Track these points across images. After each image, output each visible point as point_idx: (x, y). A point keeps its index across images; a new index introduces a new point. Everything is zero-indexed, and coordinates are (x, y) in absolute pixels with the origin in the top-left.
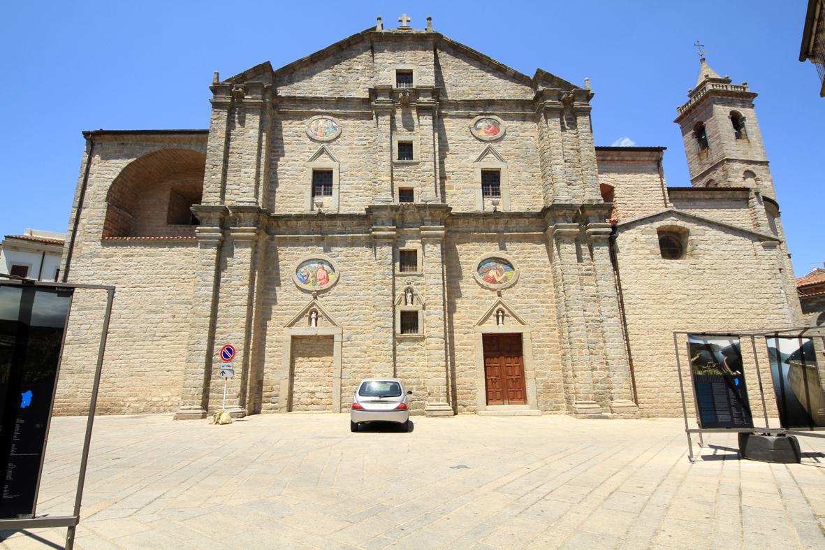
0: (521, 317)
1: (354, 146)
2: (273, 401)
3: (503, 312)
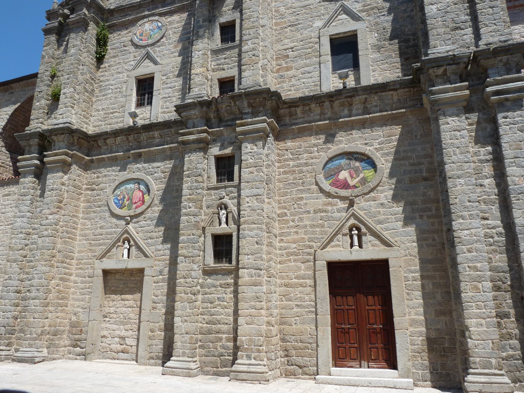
0: (386, 234)
2: (82, 345)
3: (359, 229)
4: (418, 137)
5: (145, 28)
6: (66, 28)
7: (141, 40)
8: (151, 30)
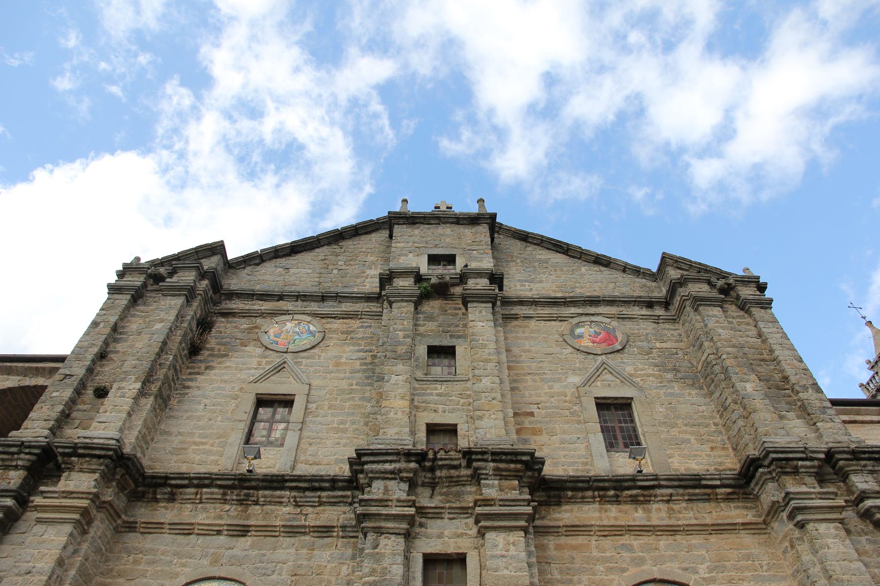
1: (343, 360)
4: (765, 568)
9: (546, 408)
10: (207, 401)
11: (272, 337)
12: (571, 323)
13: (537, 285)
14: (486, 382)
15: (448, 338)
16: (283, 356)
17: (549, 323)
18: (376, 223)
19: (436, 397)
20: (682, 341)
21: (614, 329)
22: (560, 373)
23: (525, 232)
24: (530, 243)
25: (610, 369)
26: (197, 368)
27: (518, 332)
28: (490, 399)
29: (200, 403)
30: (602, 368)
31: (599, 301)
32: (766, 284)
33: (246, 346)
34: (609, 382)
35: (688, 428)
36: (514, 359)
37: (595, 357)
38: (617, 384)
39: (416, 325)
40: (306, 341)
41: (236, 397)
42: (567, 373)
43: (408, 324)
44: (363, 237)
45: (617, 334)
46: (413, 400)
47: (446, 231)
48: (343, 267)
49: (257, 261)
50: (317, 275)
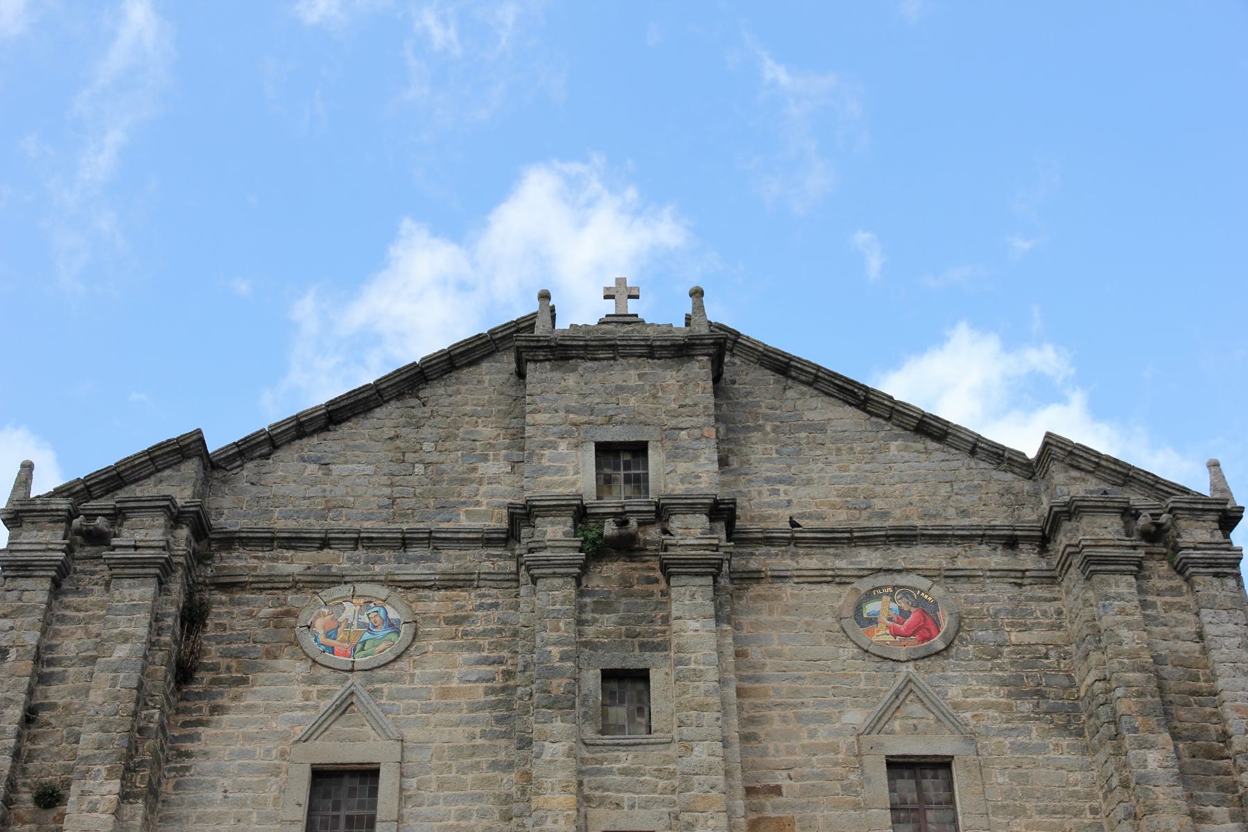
1: (454, 684)
5: (344, 616)
6: (78, 568)
7: (332, 650)
8: (365, 625)
9: (803, 777)
10: (227, 782)
11: (322, 638)
12: (856, 590)
13: (802, 492)
14: (702, 753)
15: (637, 652)
16: (347, 679)
17: (817, 589)
18: (488, 341)
19: (619, 778)
20: (1060, 627)
21: (935, 603)
22: (831, 704)
23: (784, 354)
24: (794, 378)
25: (919, 693)
26: (195, 711)
27: (759, 611)
28: (706, 787)
29: (213, 786)
30: (906, 691)
31: (915, 536)
32: (1241, 509)
33: (275, 658)
34: (915, 721)
35: (1044, 819)
36: (751, 673)
37: (896, 665)
38: (928, 725)
39: (580, 622)
40: (383, 645)
41: (276, 771)
42: (842, 702)
43: (565, 627)
44: (465, 374)
45: (940, 614)
46: (580, 784)
47: (626, 374)
48: (434, 457)
49: (265, 450)
50: (385, 480)
